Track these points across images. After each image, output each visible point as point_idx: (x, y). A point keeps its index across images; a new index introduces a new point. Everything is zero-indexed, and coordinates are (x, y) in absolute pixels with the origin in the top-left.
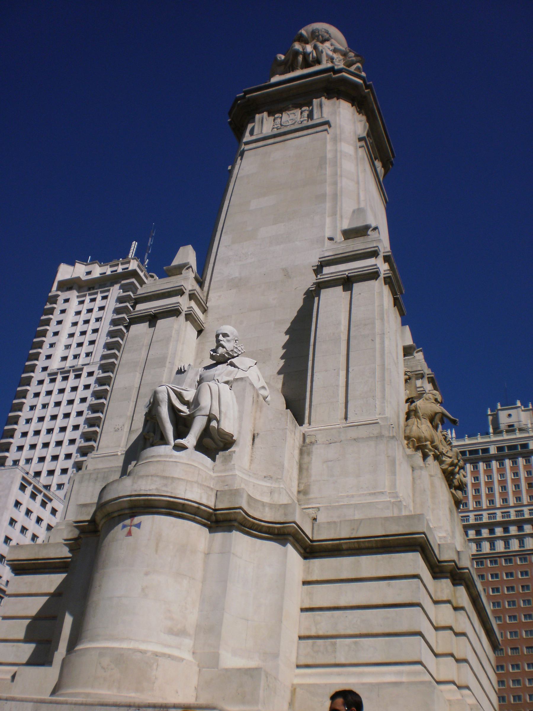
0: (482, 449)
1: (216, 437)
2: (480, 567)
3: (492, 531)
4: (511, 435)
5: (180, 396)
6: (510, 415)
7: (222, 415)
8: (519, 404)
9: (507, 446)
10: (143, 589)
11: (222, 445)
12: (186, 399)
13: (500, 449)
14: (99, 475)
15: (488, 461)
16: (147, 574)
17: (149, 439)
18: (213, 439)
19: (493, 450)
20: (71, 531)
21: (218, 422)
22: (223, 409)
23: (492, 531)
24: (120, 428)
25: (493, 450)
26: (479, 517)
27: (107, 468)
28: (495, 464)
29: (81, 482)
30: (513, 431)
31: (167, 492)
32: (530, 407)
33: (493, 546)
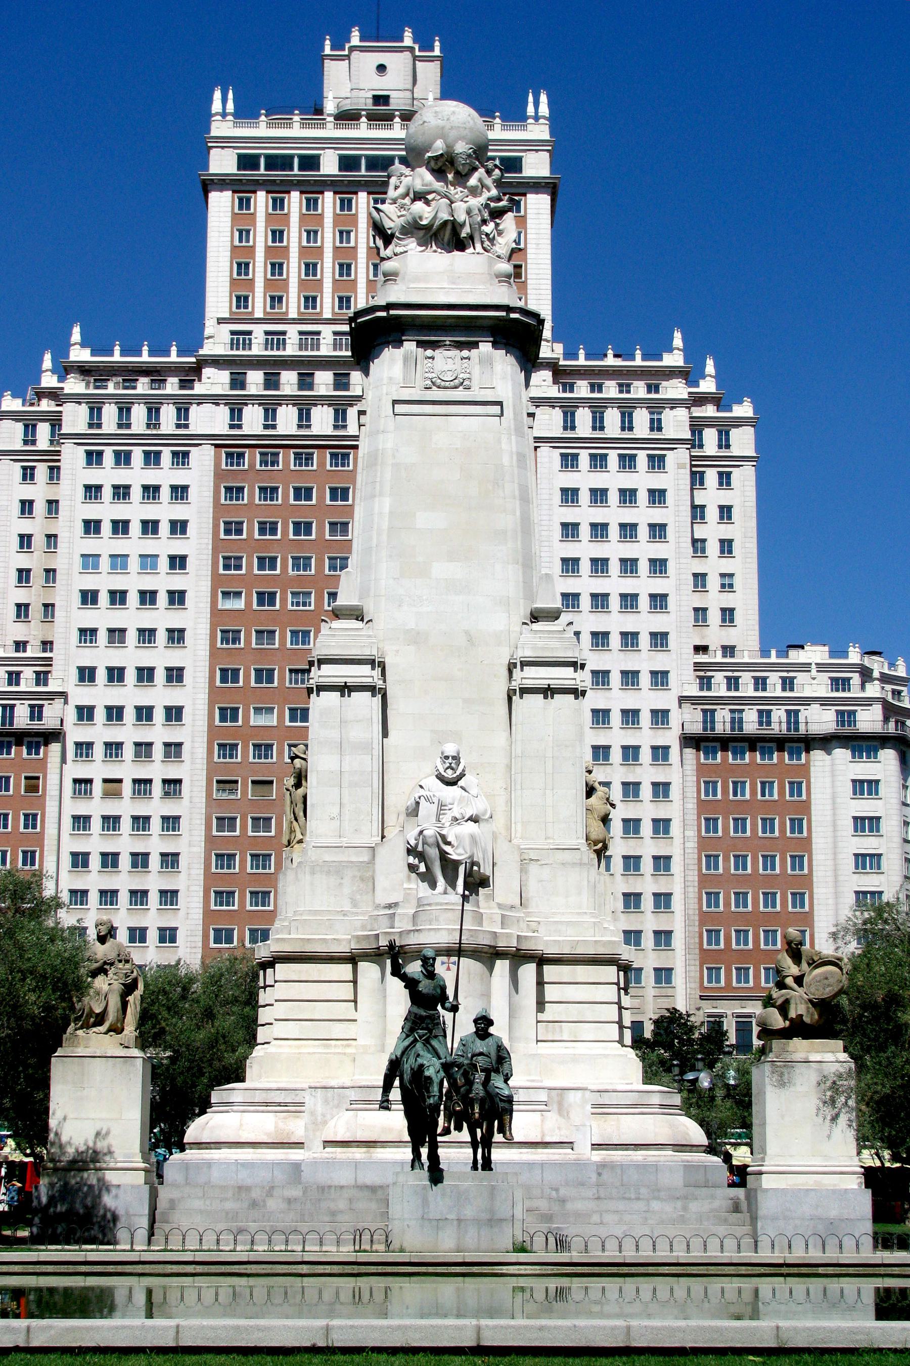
0: (301, 157)
1: (476, 876)
2: (269, 468)
3: (306, 381)
4: (378, 127)
5: (443, 837)
6: (381, 68)
8: (408, 41)
9: (367, 157)
13: (348, 163)
15: (312, 189)
19: (329, 166)
23: (306, 381)
25: (329, 166)
26: (276, 339)
28: (328, 201)
30: (388, 118)
32: (437, 52)
33: (304, 418)
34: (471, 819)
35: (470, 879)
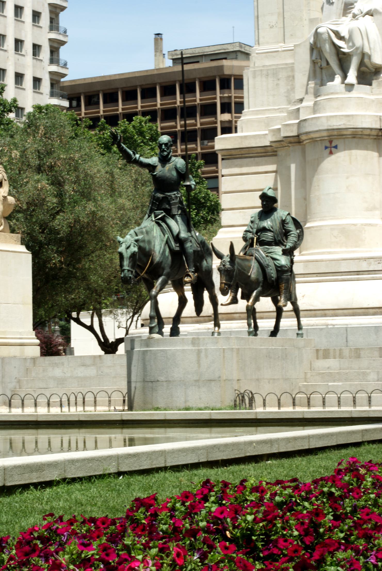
1: (369, 65)
5: (337, 34)
7: (372, 51)
10: (347, 187)
11: (374, 70)
12: (342, 35)
14: (269, 72)
16: (347, 178)
17: (317, 63)
18: (367, 67)
20: (274, 135)
21: (370, 57)
22: (372, 46)
24: (274, 25)
27: (274, 65)
29: (254, 77)
31: (351, 125)
34: (367, 13)
35: (363, 69)
